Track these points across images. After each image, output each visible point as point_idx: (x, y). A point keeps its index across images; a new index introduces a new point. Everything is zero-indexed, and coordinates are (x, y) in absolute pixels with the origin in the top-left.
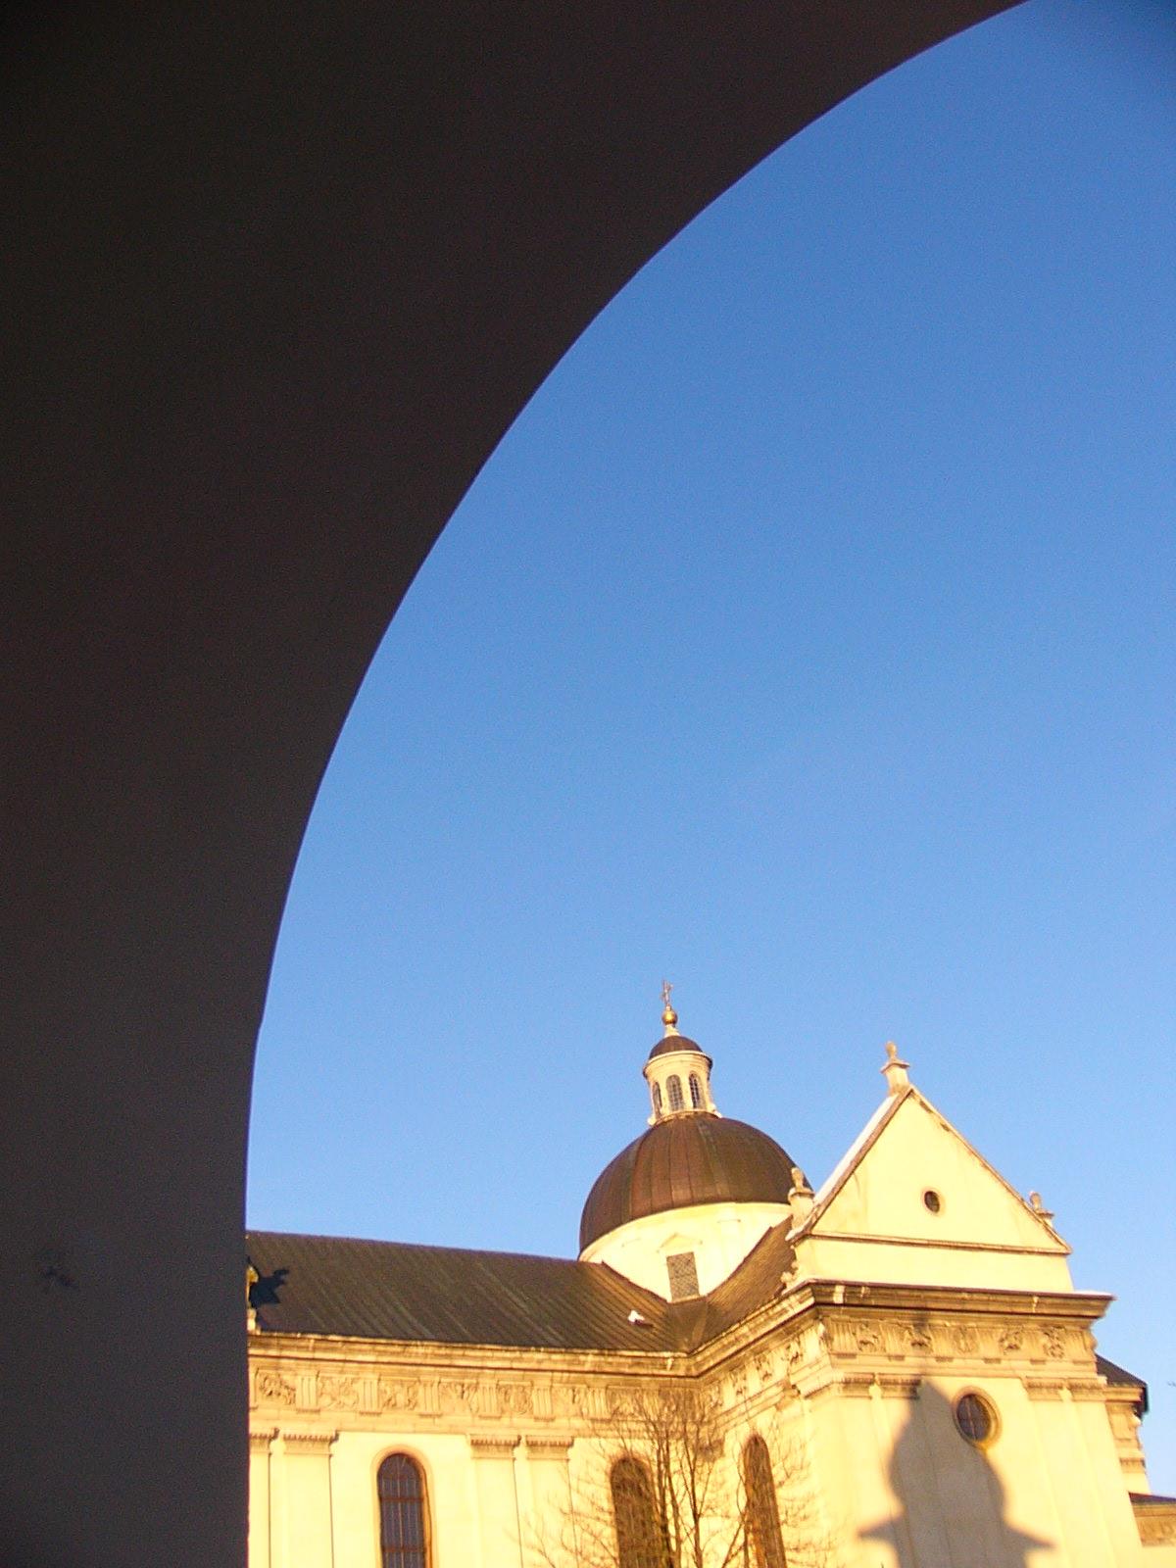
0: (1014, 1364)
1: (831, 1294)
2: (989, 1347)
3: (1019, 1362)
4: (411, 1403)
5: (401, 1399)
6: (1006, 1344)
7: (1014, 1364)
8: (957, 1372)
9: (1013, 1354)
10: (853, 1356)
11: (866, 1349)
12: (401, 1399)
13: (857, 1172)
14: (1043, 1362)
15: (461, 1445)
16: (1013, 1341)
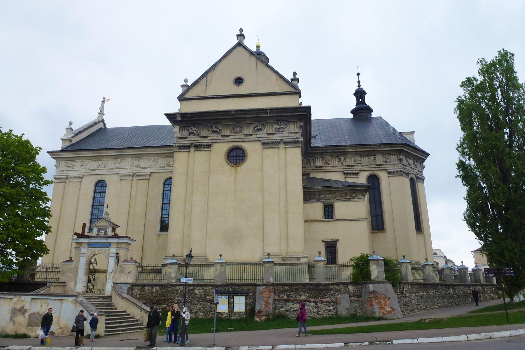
0: (258, 136)
1: (176, 118)
2: (248, 131)
3: (262, 135)
4: (105, 166)
5: (102, 166)
6: (256, 128)
7: (258, 136)
8: (230, 140)
9: (257, 133)
10: (186, 138)
11: (192, 136)
12: (102, 166)
13: (209, 75)
14: (273, 134)
15: (117, 177)
16: (260, 127)
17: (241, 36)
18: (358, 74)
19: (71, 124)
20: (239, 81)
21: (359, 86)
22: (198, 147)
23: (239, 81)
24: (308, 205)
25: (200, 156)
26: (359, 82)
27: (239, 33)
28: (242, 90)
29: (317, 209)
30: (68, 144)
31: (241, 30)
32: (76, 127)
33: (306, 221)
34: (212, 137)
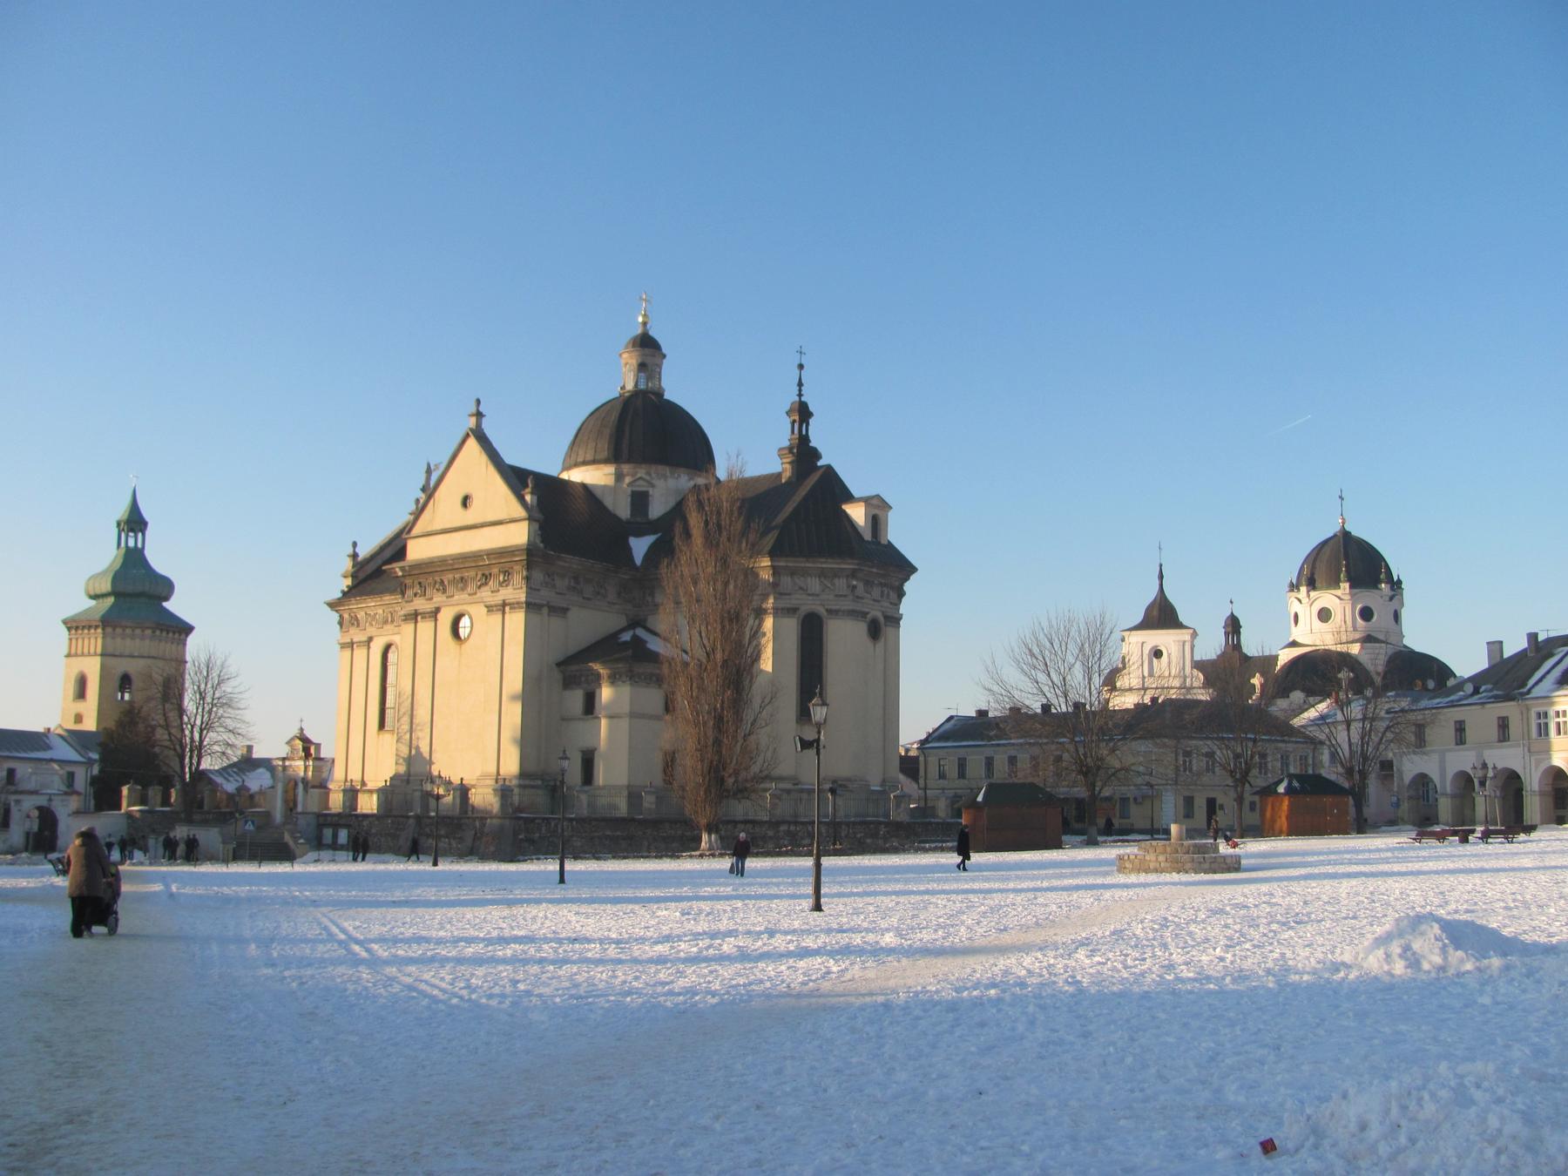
3: (485, 594)
17: (479, 415)
18: (801, 367)
19: (355, 545)
20: (466, 501)
21: (800, 395)
22: (425, 615)
23: (466, 501)
24: (568, 693)
25: (425, 627)
26: (800, 384)
27: (474, 410)
28: (470, 517)
29: (576, 698)
30: (349, 582)
31: (478, 402)
32: (364, 552)
33: (563, 719)
34: (439, 599)
